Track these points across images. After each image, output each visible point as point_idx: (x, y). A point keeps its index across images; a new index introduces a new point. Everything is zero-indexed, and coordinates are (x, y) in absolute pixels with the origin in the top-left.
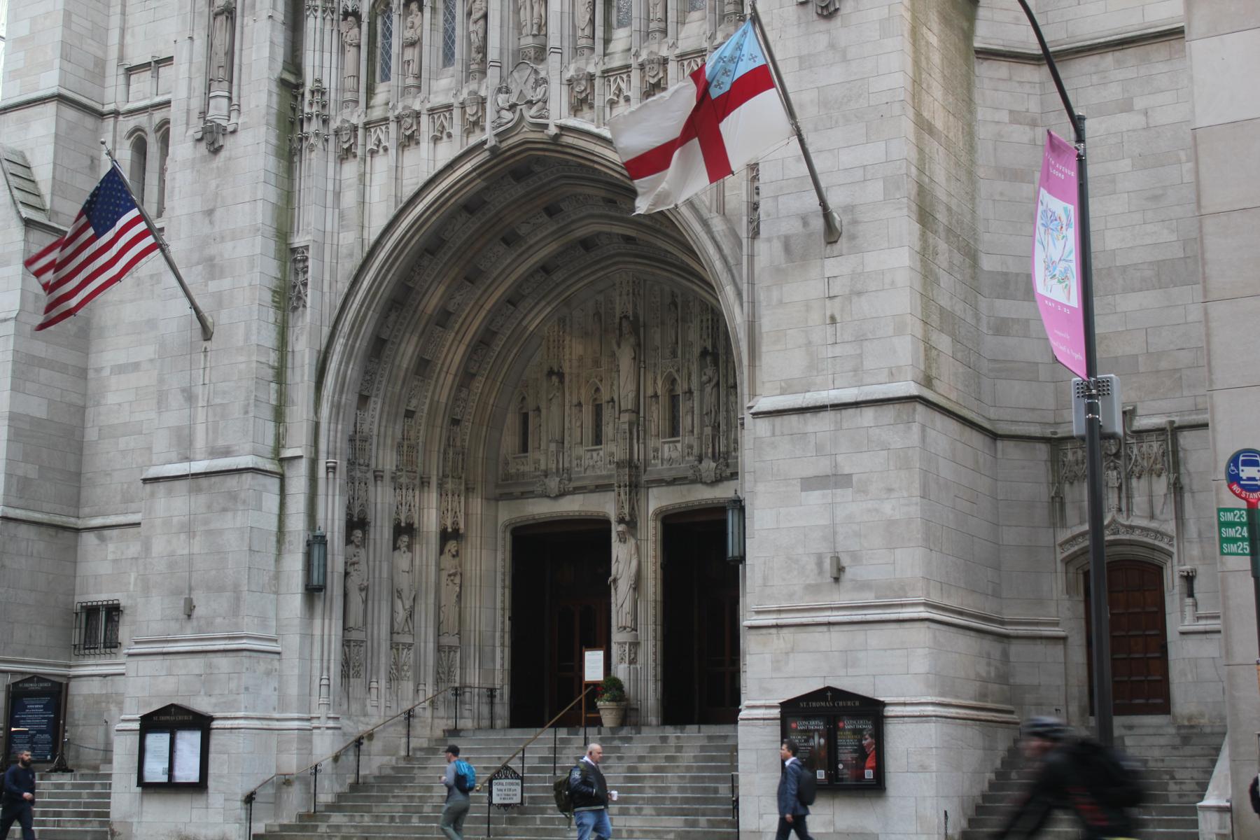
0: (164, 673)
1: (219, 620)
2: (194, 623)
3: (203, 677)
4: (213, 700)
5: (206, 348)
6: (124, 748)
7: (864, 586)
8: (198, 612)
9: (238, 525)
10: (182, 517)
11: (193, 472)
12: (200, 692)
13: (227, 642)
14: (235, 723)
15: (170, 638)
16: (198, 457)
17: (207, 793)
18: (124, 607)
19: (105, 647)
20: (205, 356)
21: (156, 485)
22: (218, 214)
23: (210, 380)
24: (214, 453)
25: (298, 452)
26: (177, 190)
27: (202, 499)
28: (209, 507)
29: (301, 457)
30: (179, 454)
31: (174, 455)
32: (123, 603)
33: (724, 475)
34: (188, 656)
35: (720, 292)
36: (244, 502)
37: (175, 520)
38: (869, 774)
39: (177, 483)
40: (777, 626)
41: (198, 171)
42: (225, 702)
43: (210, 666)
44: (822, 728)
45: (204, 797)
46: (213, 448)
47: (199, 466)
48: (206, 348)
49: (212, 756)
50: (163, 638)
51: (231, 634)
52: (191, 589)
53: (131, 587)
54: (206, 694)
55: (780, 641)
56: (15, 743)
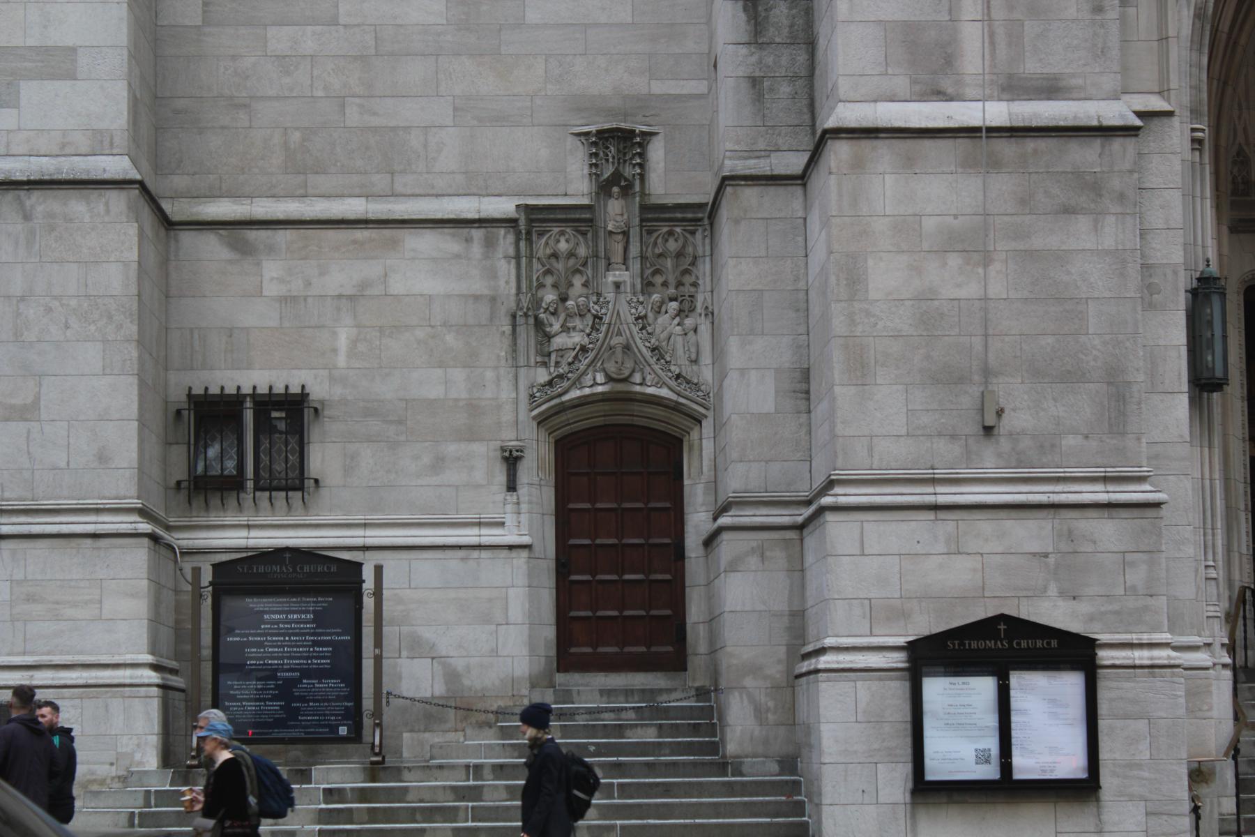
0: (941, 548)
1: (1070, 441)
2: (1005, 444)
3: (1051, 560)
4: (1084, 607)
8: (1011, 422)
9: (1108, 243)
10: (950, 219)
11: (988, 124)
12: (1045, 589)
13: (1099, 487)
14: (1162, 655)
15: (940, 473)
16: (969, 92)
17: (1098, 800)
18: (322, 402)
19: (257, 488)
21: (866, 145)
24: (1013, 88)
25: (1157, 104)
27: (1003, 185)
28: (1025, 202)
29: (1170, 114)
30: (914, 82)
31: (901, 83)
32: (318, 390)
34: (1002, 514)
36: (1121, 197)
37: (929, 224)
39: (927, 144)
42: (1117, 613)
43: (1071, 536)
45: (1090, 809)
46: (1010, 76)
47: (997, 113)
49: (1103, 724)
51: (1112, 471)
52: (987, 373)
53: (342, 360)
54: (1062, 594)
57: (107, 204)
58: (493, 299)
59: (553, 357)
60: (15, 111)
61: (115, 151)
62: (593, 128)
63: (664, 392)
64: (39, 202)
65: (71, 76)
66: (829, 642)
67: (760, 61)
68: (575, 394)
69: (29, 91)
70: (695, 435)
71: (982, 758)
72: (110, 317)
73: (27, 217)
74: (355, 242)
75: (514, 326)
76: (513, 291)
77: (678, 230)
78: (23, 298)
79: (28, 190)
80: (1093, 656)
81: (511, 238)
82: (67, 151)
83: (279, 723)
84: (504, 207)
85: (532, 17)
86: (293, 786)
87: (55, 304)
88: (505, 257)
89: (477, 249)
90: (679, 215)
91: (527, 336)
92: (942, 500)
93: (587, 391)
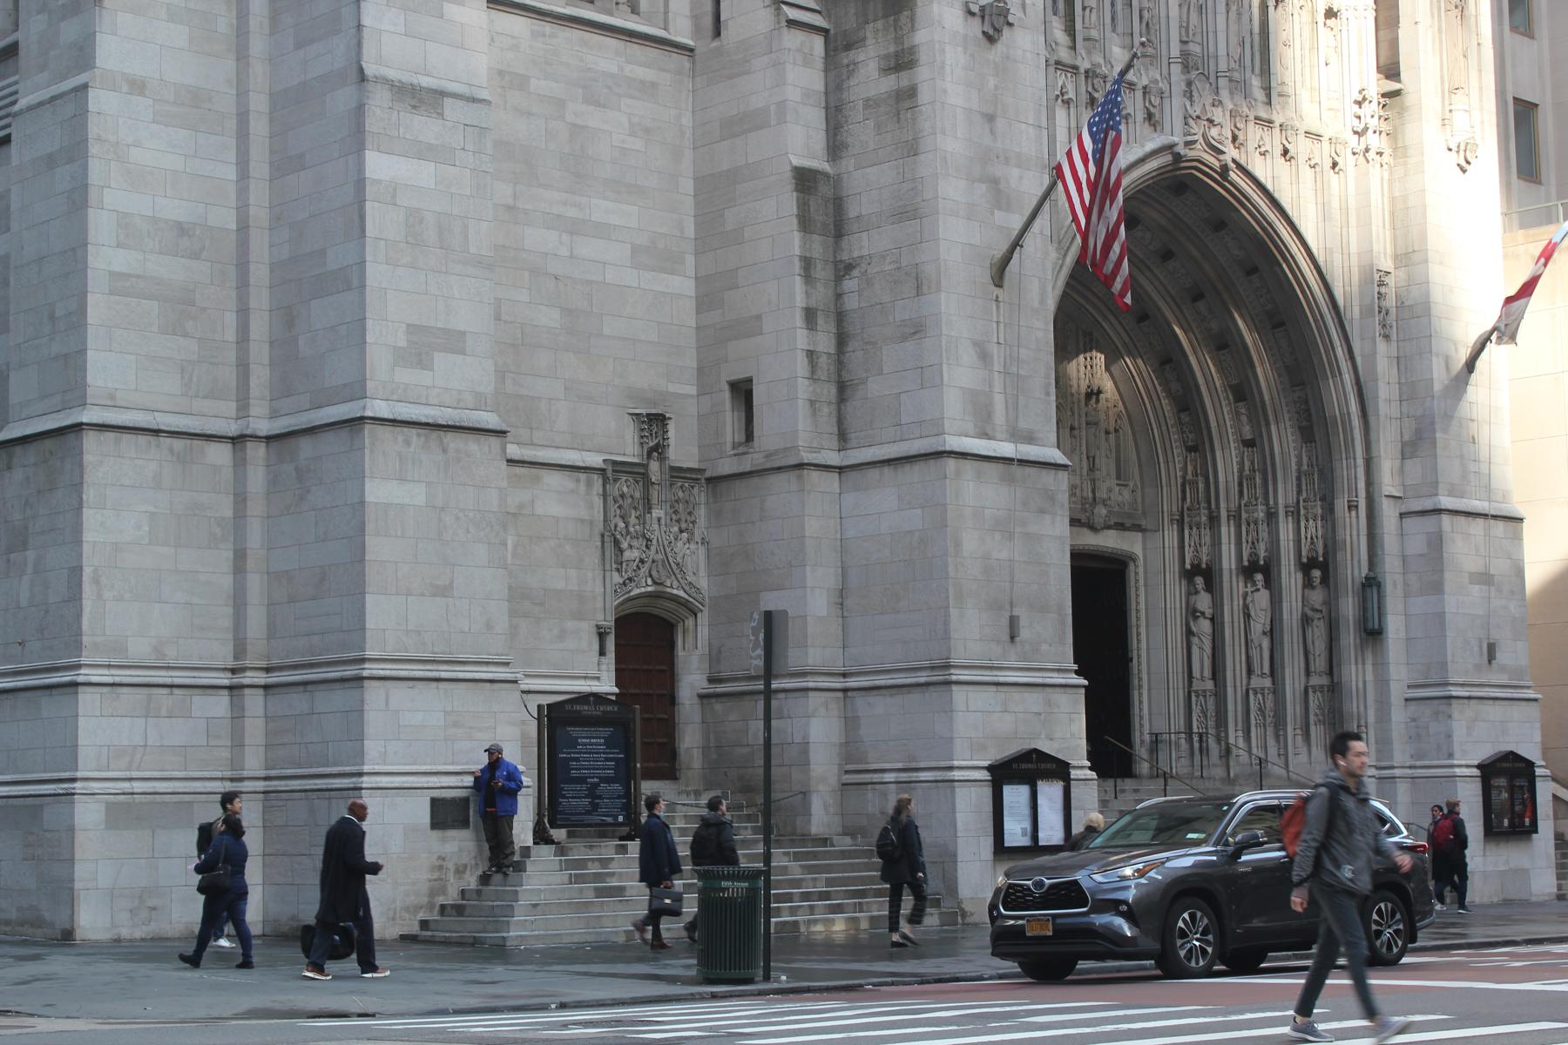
0: (998, 708)
1: (1044, 647)
3: (1042, 717)
5: (997, 297)
6: (971, 805)
7: (1503, 669)
8: (1024, 634)
11: (1018, 457)
13: (1055, 675)
20: (998, 307)
22: (1000, 123)
23: (1005, 341)
24: (1015, 436)
26: (948, 69)
31: (970, 427)
34: (1023, 689)
35: (1333, 376)
38: (1527, 821)
40: (1469, 698)
41: (972, 56)
44: (1505, 784)
48: (997, 297)
50: (986, 663)
55: (1471, 709)
56: (564, 797)
57: (490, 446)
58: (592, 523)
59: (624, 565)
60: (431, 373)
61: (488, 409)
62: (644, 411)
63: (682, 593)
64: (450, 439)
65: (463, 352)
66: (956, 763)
67: (814, 391)
68: (636, 591)
69: (440, 360)
70: (690, 622)
71: (1024, 834)
72: (492, 527)
73: (445, 451)
74: (516, 475)
75: (603, 542)
76: (602, 518)
77: (686, 485)
78: (443, 509)
79: (445, 431)
80: (1069, 774)
81: (600, 481)
82: (461, 405)
83: (588, 813)
84: (596, 460)
85: (606, 331)
86: (739, 852)
87: (461, 515)
88: (598, 494)
89: (582, 487)
90: (688, 475)
91: (610, 548)
92: (1002, 679)
93: (643, 590)
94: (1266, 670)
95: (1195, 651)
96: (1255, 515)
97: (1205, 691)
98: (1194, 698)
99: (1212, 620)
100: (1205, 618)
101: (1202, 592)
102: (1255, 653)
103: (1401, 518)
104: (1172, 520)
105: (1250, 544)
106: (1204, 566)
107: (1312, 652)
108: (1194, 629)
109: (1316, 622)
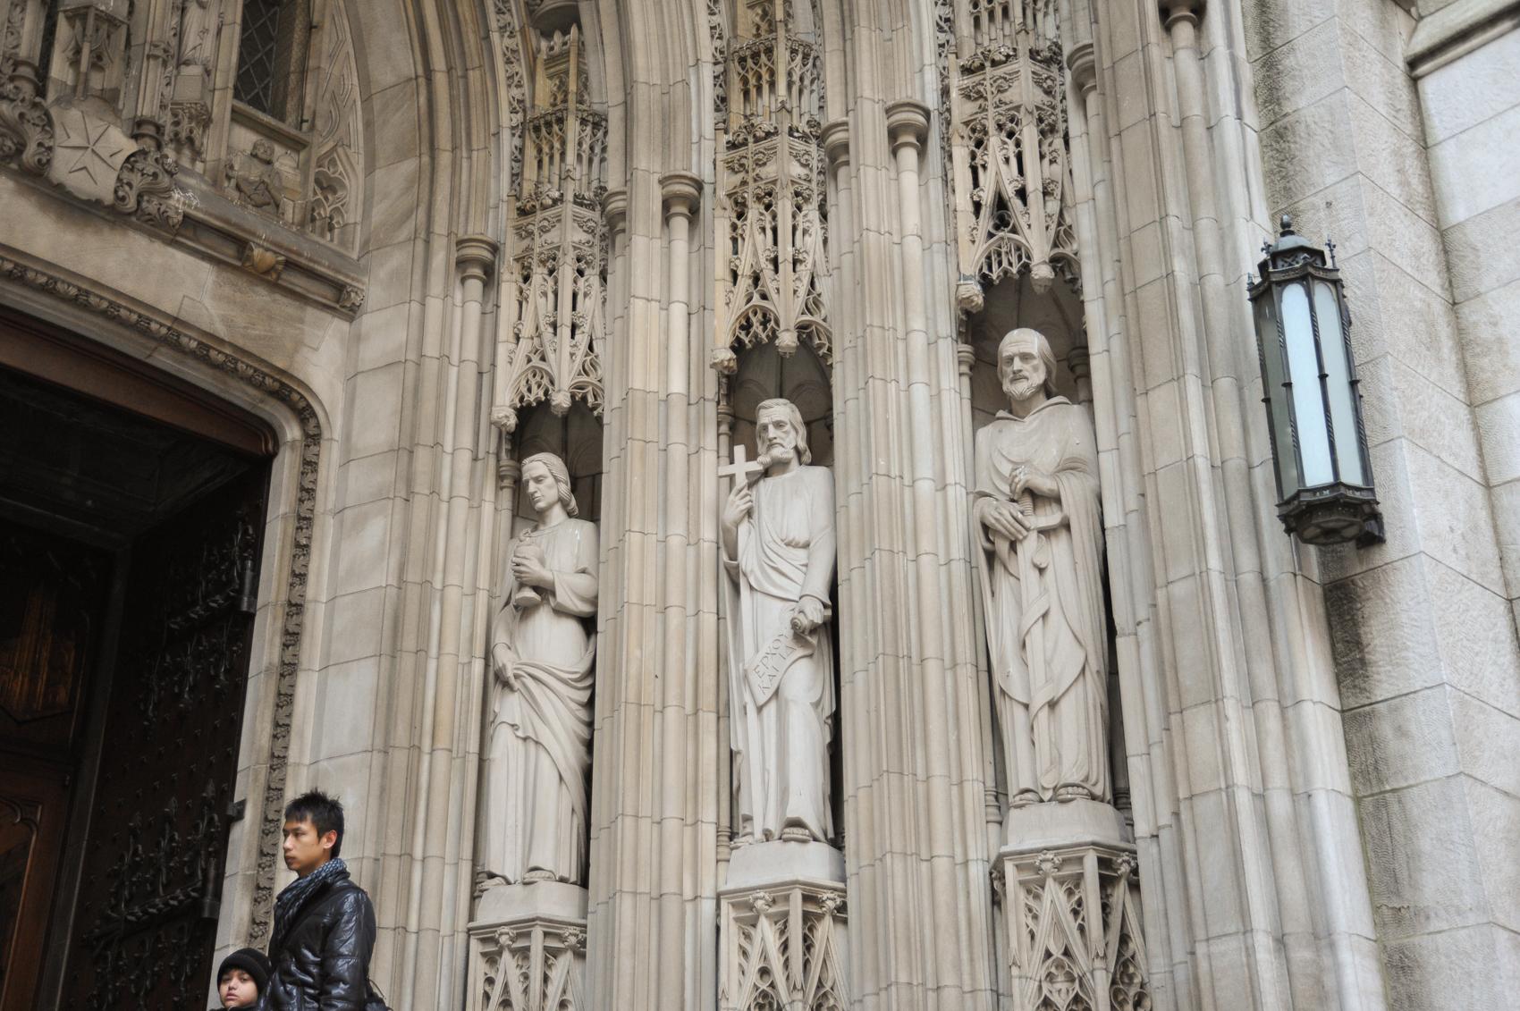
33: (151, 206)
94: (808, 802)
95: (504, 745)
96: (769, 171)
97: (523, 928)
98: (479, 967)
99: (589, 624)
100: (560, 612)
101: (557, 514)
102: (753, 736)
103: (1414, 81)
104: (462, 263)
105: (744, 283)
106: (561, 400)
107: (1017, 691)
108: (505, 658)
109: (1030, 548)
